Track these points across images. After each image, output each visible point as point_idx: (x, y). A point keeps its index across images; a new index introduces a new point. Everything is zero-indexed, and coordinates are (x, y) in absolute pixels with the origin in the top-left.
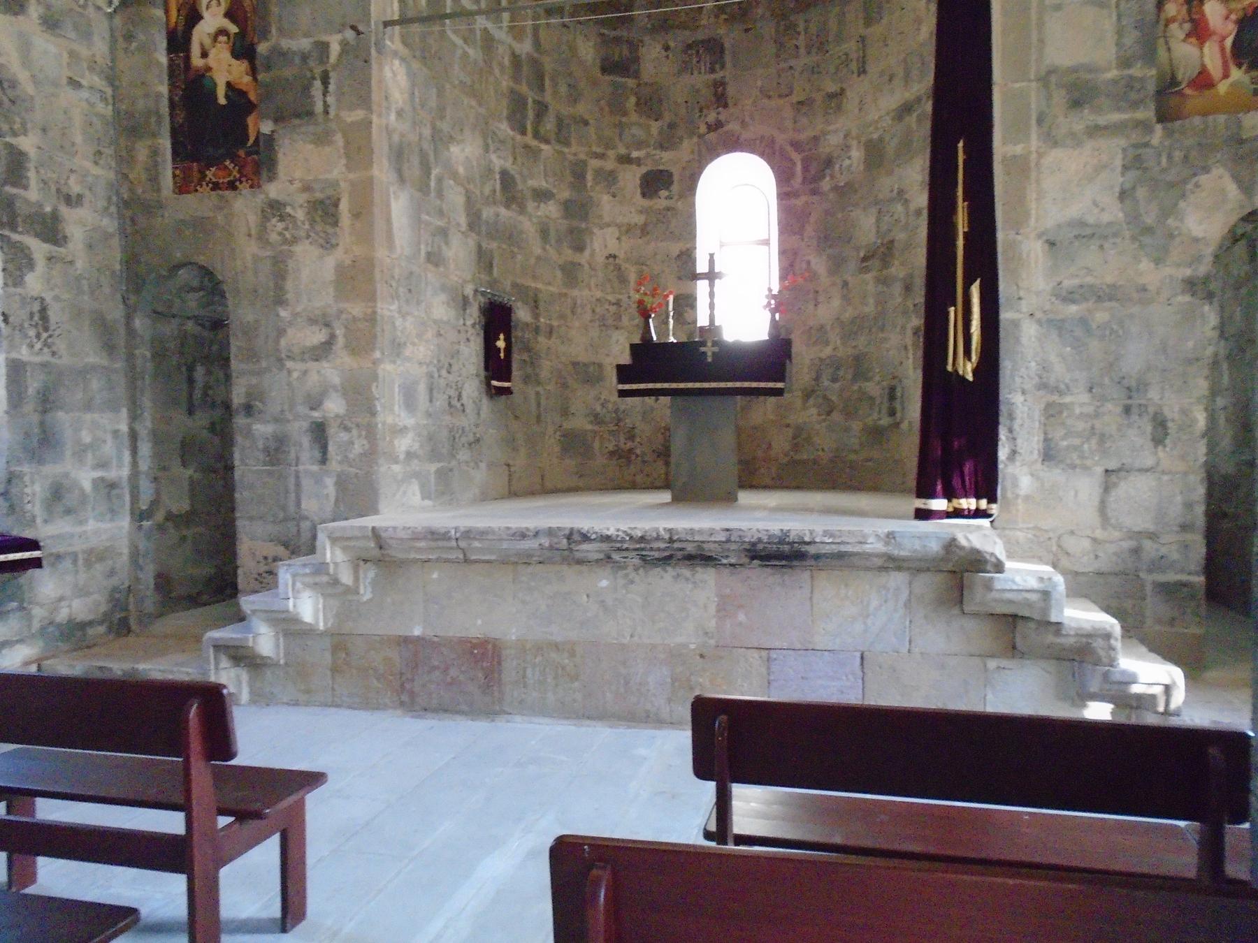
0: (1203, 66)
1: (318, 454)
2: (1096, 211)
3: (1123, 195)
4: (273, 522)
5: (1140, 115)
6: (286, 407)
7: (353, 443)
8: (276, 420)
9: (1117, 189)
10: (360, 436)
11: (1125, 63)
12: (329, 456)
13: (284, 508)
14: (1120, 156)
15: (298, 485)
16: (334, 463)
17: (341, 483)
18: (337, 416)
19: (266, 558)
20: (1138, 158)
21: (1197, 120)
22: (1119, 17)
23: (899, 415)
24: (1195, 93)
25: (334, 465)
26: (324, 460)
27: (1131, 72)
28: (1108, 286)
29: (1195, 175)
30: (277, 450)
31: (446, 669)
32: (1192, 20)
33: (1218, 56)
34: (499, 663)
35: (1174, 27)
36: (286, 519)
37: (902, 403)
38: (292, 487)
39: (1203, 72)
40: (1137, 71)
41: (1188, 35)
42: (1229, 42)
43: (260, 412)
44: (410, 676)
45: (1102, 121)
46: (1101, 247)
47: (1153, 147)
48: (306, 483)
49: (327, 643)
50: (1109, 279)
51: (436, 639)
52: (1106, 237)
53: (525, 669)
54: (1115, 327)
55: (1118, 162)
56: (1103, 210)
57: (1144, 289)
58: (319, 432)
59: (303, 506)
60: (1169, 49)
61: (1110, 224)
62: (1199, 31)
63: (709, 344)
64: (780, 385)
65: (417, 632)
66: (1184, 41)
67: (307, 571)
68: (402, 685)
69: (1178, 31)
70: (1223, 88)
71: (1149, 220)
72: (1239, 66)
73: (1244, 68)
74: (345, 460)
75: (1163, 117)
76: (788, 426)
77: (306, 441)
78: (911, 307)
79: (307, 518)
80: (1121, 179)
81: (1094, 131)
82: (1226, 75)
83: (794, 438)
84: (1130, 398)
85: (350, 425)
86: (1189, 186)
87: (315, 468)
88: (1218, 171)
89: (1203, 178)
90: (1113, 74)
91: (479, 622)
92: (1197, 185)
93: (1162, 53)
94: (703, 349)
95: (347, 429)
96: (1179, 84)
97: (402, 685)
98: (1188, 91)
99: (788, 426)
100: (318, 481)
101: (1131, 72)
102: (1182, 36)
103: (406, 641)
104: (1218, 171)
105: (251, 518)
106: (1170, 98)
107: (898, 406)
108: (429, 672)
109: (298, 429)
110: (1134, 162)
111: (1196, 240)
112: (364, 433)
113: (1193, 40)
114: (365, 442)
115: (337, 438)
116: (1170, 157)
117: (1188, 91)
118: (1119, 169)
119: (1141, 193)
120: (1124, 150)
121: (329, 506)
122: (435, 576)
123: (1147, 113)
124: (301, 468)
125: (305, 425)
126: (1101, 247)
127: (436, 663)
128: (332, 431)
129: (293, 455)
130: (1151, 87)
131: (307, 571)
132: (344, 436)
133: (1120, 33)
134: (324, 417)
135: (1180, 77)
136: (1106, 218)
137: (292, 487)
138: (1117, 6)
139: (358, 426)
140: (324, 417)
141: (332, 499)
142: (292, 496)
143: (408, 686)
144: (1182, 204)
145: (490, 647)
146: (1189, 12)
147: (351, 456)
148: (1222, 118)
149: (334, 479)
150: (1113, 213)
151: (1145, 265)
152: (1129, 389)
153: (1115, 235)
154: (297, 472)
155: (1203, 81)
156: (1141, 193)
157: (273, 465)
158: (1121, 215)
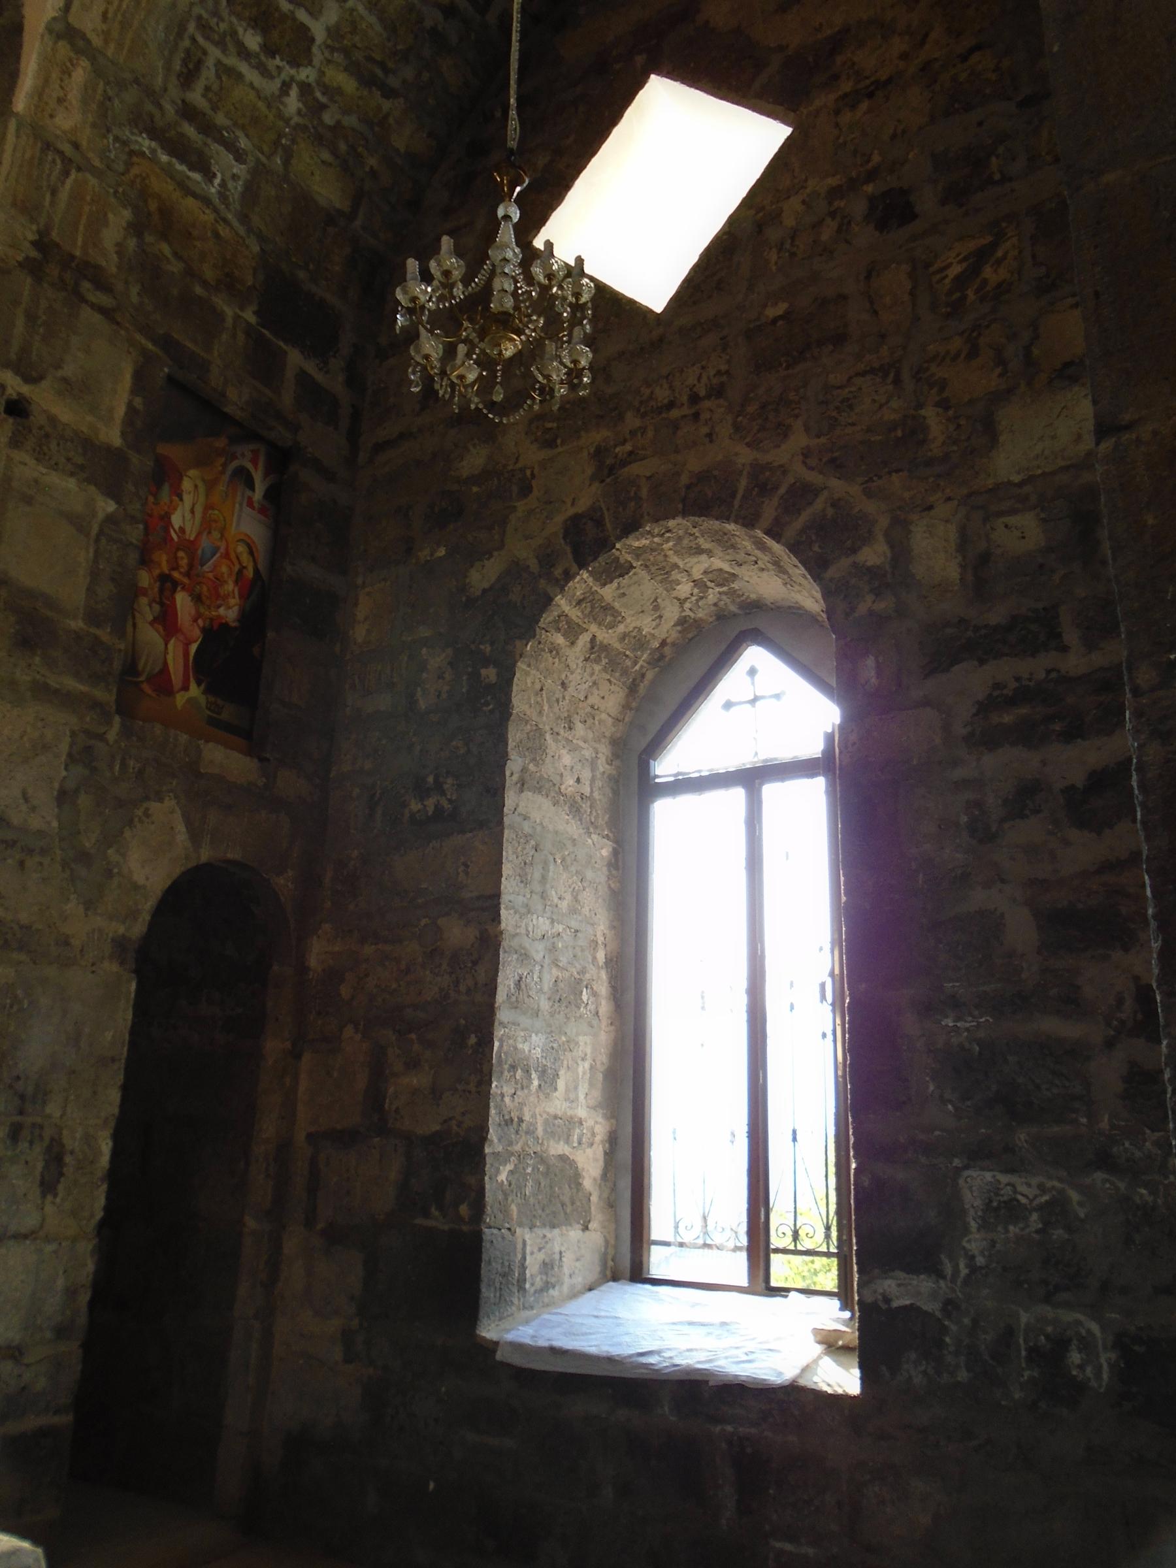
0: (165, 663)
2: (24, 808)
3: (64, 797)
5: (99, 694)
9: (56, 785)
11: (93, 617)
14: (68, 739)
20: (88, 749)
21: (158, 729)
22: (96, 552)
24: (154, 695)
27: (98, 632)
28: (21, 927)
29: (147, 798)
32: (162, 604)
33: (181, 661)
35: (144, 601)
39: (165, 669)
40: (104, 634)
41: (155, 620)
42: (194, 648)
45: (53, 682)
46: (21, 864)
47: (108, 744)
50: (24, 917)
52: (30, 852)
54: (19, 992)
55: (64, 747)
56: (33, 809)
57: (66, 942)
60: (134, 625)
61: (40, 833)
62: (167, 621)
66: (152, 623)
69: (146, 610)
70: (180, 699)
71: (88, 842)
72: (199, 684)
73: (203, 686)
75: (125, 708)
80: (64, 773)
81: (42, 691)
82: (185, 688)
84: (21, 1112)
86: (139, 812)
88: (169, 803)
89: (154, 806)
90: (77, 624)
92: (147, 814)
93: (129, 629)
96: (138, 674)
98: (146, 688)
101: (98, 632)
102: (151, 618)
104: (169, 803)
106: (133, 688)
110: (82, 755)
111: (136, 887)
113: (161, 628)
116: (124, 764)
117: (146, 688)
118: (64, 758)
119: (84, 801)
120: (73, 734)
123: (106, 695)
126: (21, 864)
130: (117, 665)
133: (94, 574)
135: (140, 667)
136: (35, 823)
138: (97, 540)
144: (127, 833)
146: (161, 591)
148: (184, 738)
150: (44, 818)
151: (73, 906)
152: (22, 1097)
153: (43, 852)
155: (162, 682)
156: (84, 801)
158: (55, 824)
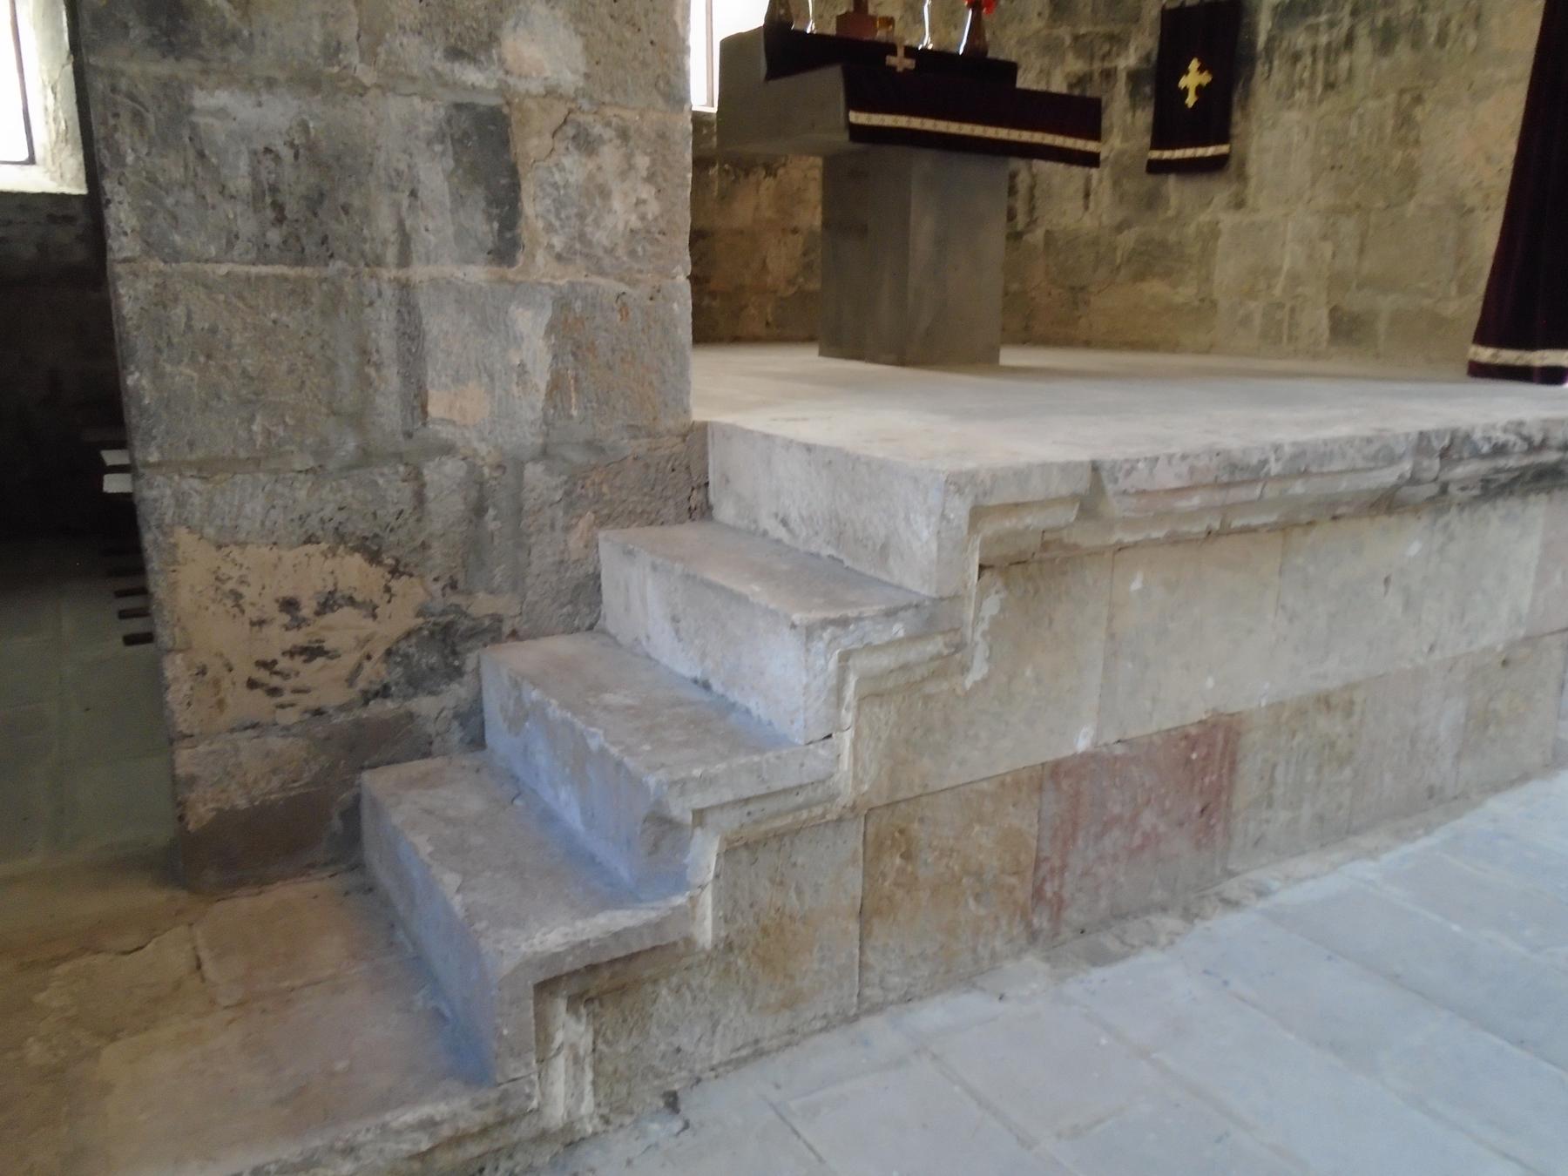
1: (483, 228)
4: (317, 473)
6: (349, 33)
7: (605, 193)
8: (309, 82)
10: (628, 168)
12: (525, 237)
13: (357, 420)
15: (411, 334)
16: (541, 257)
17: (568, 329)
18: (551, 93)
19: (289, 605)
23: (1021, 220)
25: (540, 265)
26: (505, 250)
30: (315, 201)
31: (1135, 818)
34: (1233, 768)
36: (366, 458)
37: (1032, 197)
38: (386, 343)
43: (228, 38)
44: (1057, 863)
48: (439, 324)
49: (852, 840)
51: (1119, 750)
53: (1274, 766)
58: (486, 145)
59: (434, 410)
63: (901, 52)
64: (1091, 146)
65: (1082, 744)
67: (899, 630)
68: (1038, 894)
74: (580, 250)
76: (795, 231)
77: (435, 175)
78: (1068, 41)
79: (448, 449)
83: (805, 254)
85: (597, 129)
87: (478, 274)
91: (1210, 683)
94: (891, 60)
95: (586, 143)
97: (1038, 894)
99: (795, 231)
100: (488, 318)
103: (1056, 771)
105: (206, 469)
107: (1021, 207)
108: (1099, 837)
109: (400, 127)
112: (642, 162)
114: (647, 192)
115: (550, 172)
121: (531, 405)
122: (1136, 585)
124: (419, 272)
125: (430, 113)
127: (1117, 809)
128: (531, 145)
129: (385, 224)
131: (899, 630)
132: (574, 167)
134: (503, 89)
137: (386, 343)
139: (624, 135)
140: (503, 89)
141: (541, 380)
142: (391, 379)
143: (1049, 890)
145: (1220, 737)
147: (600, 237)
149: (547, 314)
154: (405, 287)
157: (300, 261)
